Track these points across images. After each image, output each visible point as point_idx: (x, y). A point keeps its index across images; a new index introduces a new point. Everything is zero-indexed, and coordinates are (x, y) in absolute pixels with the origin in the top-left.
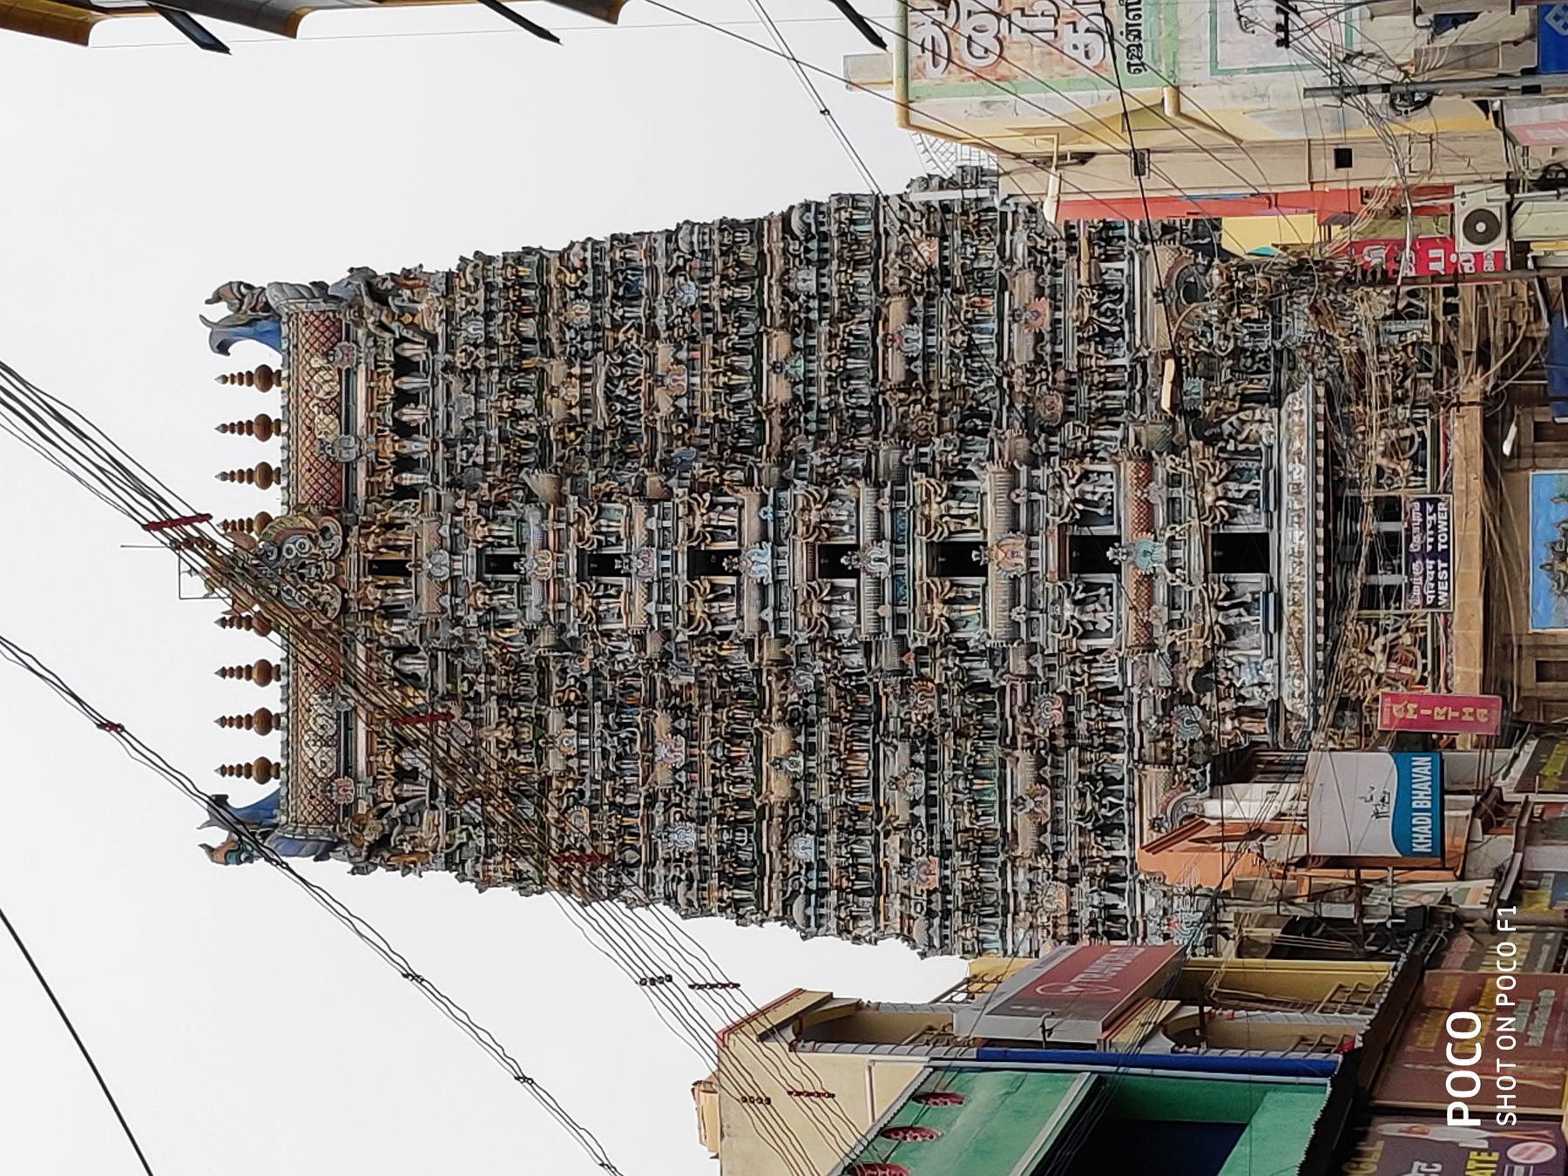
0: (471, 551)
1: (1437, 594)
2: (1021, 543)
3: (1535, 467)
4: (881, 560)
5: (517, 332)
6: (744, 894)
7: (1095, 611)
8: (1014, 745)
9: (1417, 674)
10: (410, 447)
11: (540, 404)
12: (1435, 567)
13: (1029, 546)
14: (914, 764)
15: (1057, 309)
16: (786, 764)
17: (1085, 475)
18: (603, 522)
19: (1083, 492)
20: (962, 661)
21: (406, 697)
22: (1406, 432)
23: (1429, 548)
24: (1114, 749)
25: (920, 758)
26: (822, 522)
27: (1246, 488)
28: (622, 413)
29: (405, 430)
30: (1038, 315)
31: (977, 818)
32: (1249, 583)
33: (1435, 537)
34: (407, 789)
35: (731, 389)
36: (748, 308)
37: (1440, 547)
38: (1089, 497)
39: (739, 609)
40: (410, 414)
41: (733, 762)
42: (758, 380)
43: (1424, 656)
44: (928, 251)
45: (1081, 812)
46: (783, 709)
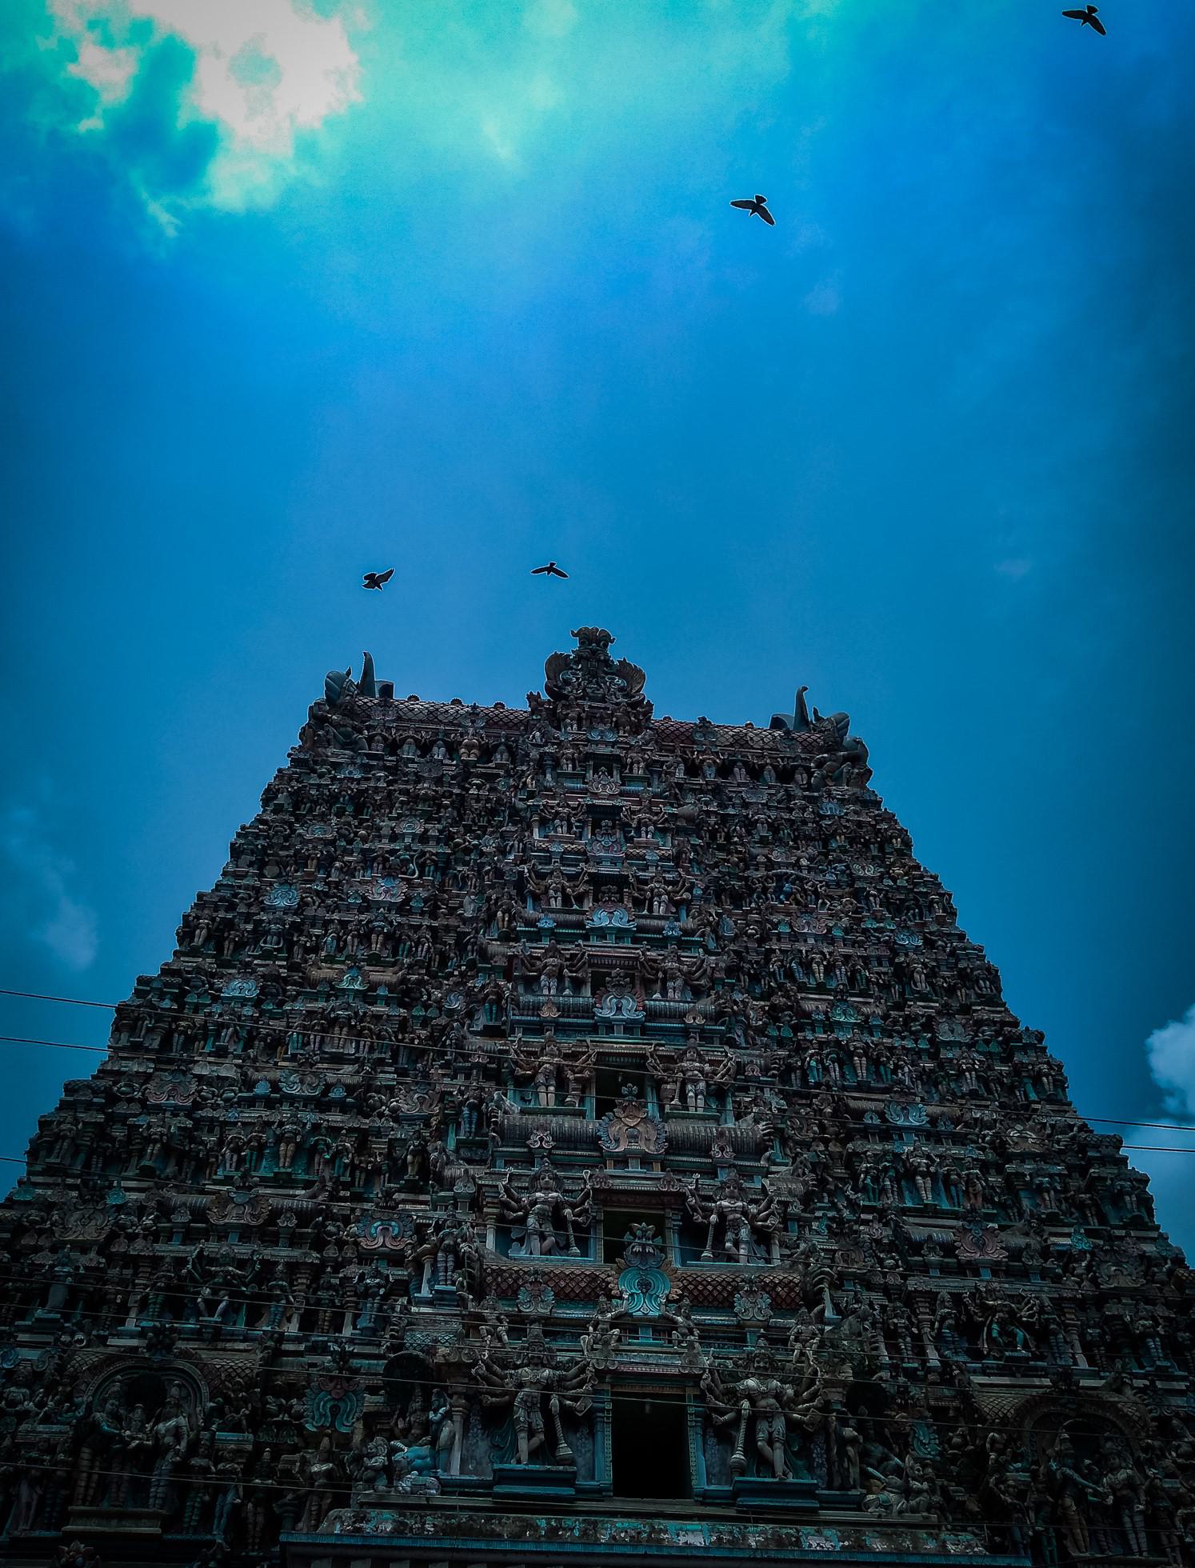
0: (617, 751)
2: (651, 1149)
4: (619, 1009)
5: (833, 835)
6: (198, 941)
7: (543, 1237)
8: (334, 1197)
10: (711, 775)
11: (763, 841)
13: (646, 1160)
14: (329, 1087)
15: (995, 1273)
16: (354, 972)
17: (762, 1237)
18: (651, 828)
19: (736, 1226)
20: (472, 1107)
21: (469, 747)
24: (308, 1322)
25: (337, 1094)
26: (665, 972)
27: (778, 1456)
29: (725, 770)
30: (981, 1246)
31: (237, 1150)
32: (596, 1459)
34: (378, 749)
35: (807, 966)
36: (902, 994)
38: (730, 1235)
39: (553, 911)
40: (740, 774)
41: (365, 938)
42: (821, 989)
44: (1023, 1137)
45: (212, 1261)
46: (420, 983)
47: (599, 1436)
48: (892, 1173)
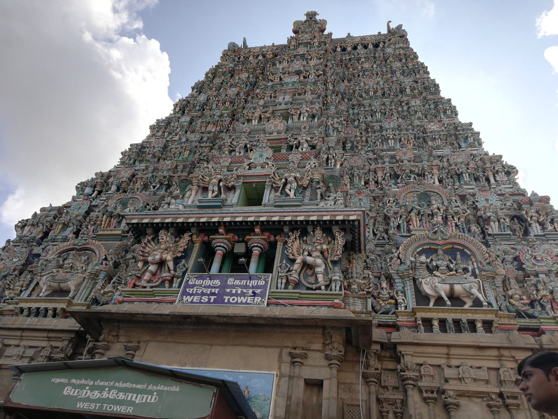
1: (191, 295)
3: (281, 376)
7: (240, 153)
9: (143, 283)
12: (213, 294)
18: (315, 58)
21: (269, 55)
22: (320, 278)
23: (228, 290)
27: (292, 194)
28: (359, 76)
29: (355, 48)
33: (236, 295)
35: (367, 93)
37: (226, 298)
43: (152, 287)
47: (236, 193)
48: (380, 140)
